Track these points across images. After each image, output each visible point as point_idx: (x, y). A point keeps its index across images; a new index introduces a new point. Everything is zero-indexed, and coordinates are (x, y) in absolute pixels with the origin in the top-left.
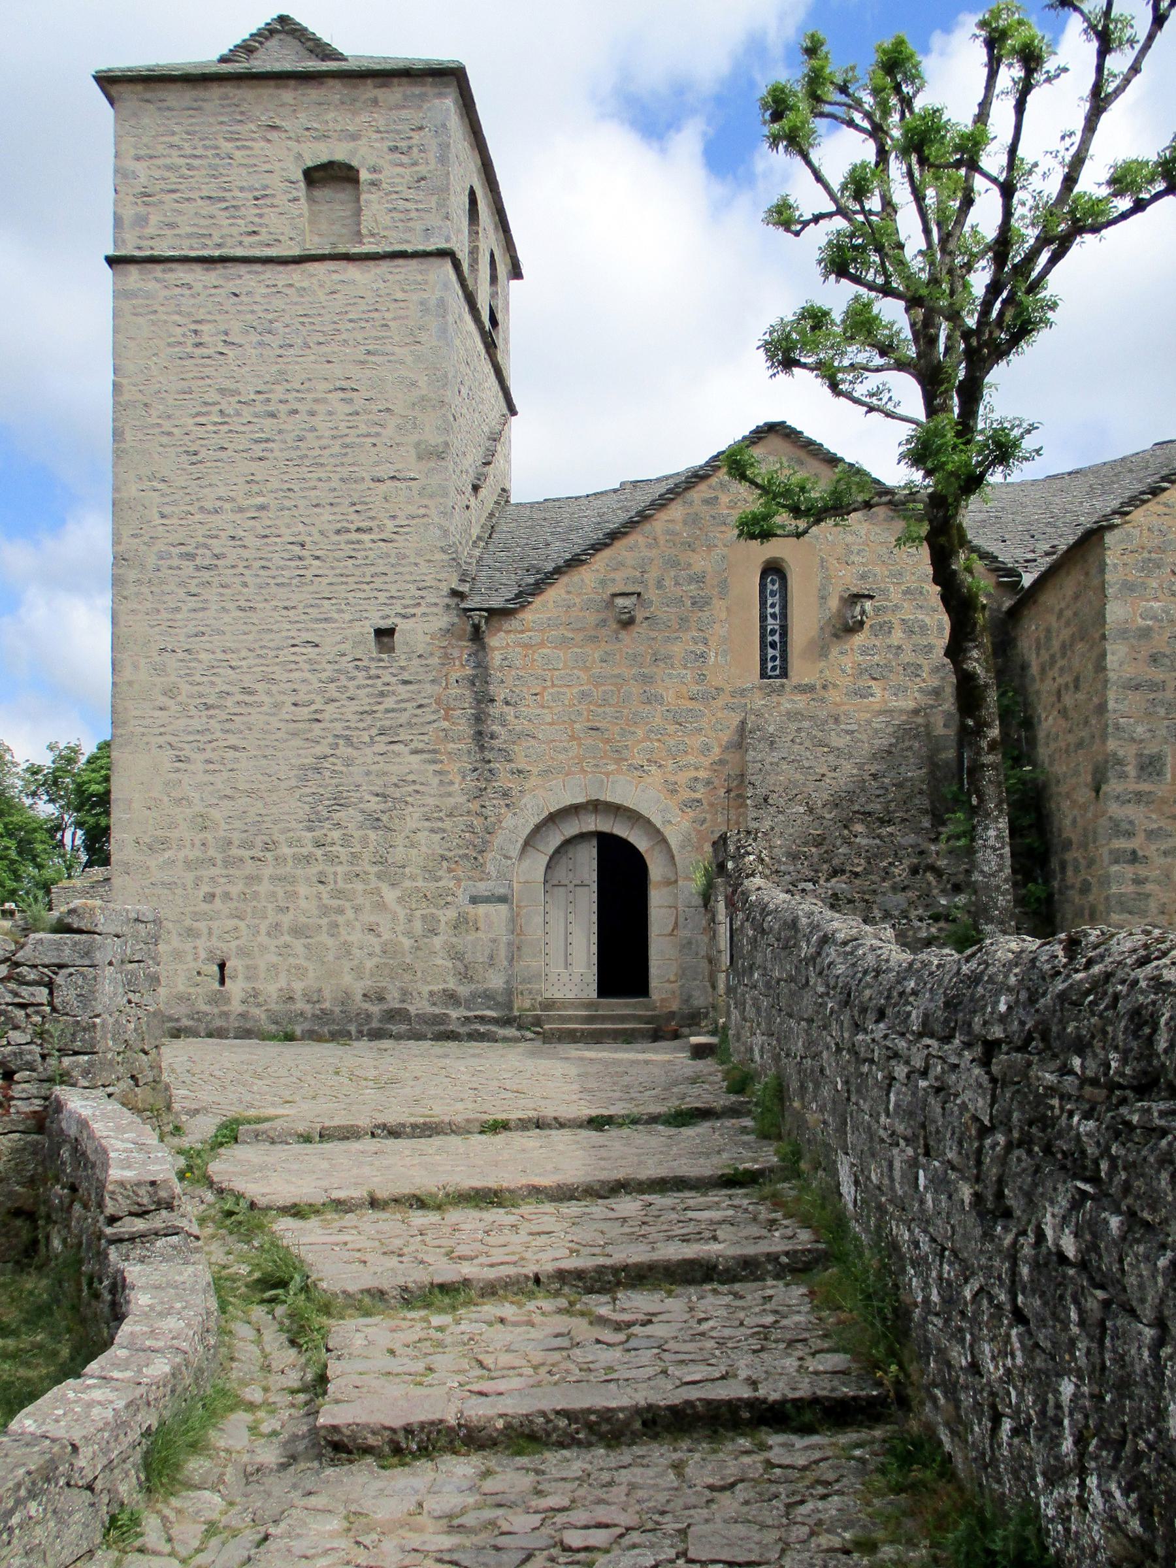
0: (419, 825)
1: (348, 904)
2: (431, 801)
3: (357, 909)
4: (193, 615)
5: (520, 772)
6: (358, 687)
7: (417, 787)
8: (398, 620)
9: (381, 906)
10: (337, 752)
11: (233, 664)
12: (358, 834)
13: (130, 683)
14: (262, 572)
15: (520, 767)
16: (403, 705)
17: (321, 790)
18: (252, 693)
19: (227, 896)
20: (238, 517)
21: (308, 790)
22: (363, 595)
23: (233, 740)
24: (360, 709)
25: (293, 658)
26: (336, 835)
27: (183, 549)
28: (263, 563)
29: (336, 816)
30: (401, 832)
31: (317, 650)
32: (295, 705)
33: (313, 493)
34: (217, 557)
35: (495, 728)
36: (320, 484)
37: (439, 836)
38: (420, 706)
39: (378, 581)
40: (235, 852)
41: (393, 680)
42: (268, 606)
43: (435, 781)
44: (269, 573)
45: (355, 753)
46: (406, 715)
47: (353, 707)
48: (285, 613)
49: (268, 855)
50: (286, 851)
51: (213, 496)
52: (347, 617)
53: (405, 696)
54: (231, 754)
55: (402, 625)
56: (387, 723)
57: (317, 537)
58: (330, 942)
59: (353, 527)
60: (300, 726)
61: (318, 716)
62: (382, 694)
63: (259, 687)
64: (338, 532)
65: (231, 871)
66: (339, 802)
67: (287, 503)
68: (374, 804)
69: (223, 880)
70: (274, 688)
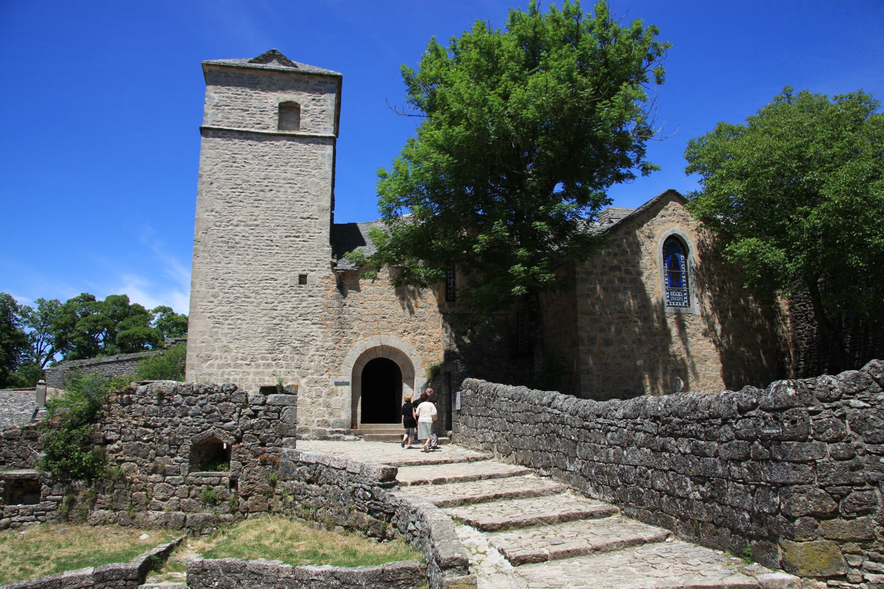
0: (315, 353)
6: (292, 297)
7: (314, 338)
10: (282, 322)
12: (289, 356)
14: (255, 250)
20: (247, 229)
21: (270, 338)
23: (240, 316)
25: (267, 285)
26: (281, 356)
29: (282, 348)
30: (307, 355)
33: (277, 221)
34: (237, 243)
39: (301, 256)
40: (239, 362)
43: (321, 336)
45: (290, 323)
47: (290, 305)
49: (253, 363)
50: (260, 362)
51: (237, 220)
53: (310, 302)
54: (239, 321)
56: (303, 312)
59: (293, 235)
62: (302, 301)
64: (286, 237)
65: (235, 370)
66: (282, 343)
68: (297, 344)
70: (258, 297)
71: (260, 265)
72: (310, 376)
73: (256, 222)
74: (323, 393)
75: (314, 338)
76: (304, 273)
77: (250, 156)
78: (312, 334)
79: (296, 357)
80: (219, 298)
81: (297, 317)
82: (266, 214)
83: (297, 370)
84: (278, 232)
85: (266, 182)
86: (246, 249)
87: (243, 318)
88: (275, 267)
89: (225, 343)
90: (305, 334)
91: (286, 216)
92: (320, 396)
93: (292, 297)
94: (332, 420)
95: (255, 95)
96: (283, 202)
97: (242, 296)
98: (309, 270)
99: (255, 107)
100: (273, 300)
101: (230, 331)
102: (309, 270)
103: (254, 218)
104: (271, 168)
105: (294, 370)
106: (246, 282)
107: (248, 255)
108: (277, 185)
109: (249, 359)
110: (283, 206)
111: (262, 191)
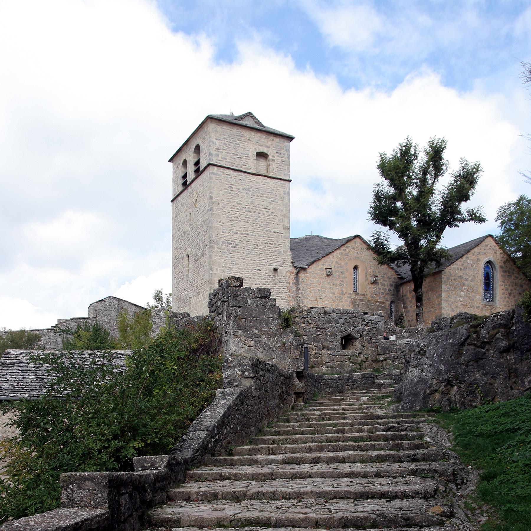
6: (270, 282)
34: (236, 245)
39: (275, 257)
42: (249, 259)
52: (268, 265)
73: (247, 232)
76: (276, 267)
77: (241, 188)
85: (251, 207)
86: (242, 249)
91: (265, 230)
93: (270, 282)
95: (241, 144)
99: (242, 153)
103: (246, 229)
107: (243, 253)
111: (250, 212)
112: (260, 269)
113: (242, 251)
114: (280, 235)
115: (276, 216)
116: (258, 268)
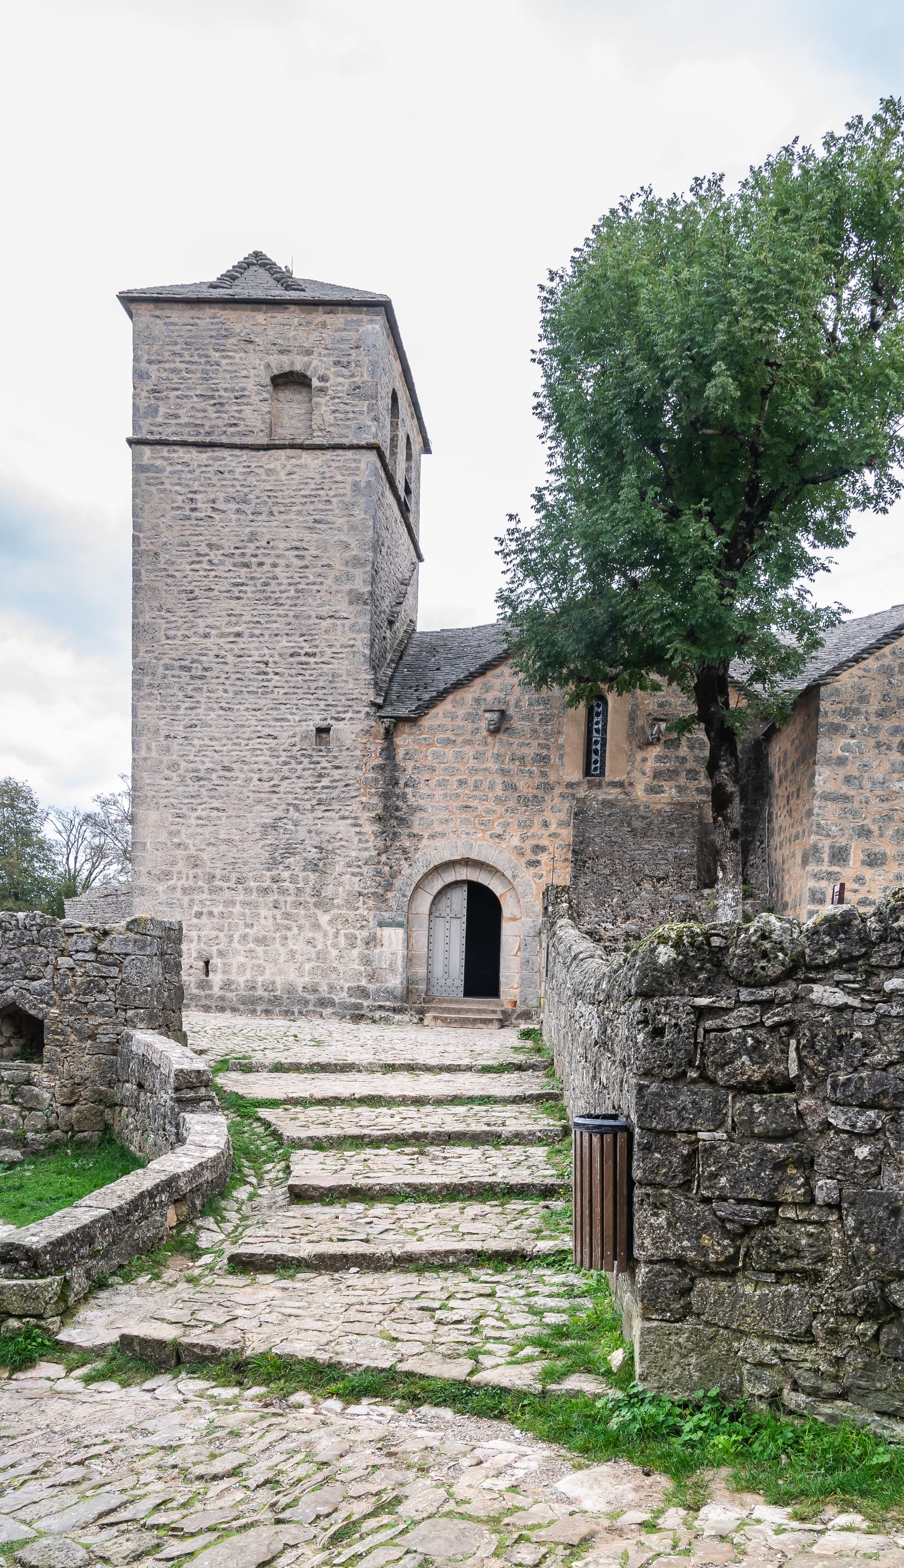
1: (294, 924)
2: (353, 854)
3: (300, 928)
4: (189, 712)
5: (415, 836)
6: (304, 770)
7: (343, 843)
8: (332, 722)
9: (316, 926)
10: (289, 816)
11: (217, 748)
12: (301, 875)
13: (145, 759)
14: (238, 682)
15: (415, 832)
16: (335, 784)
17: (277, 842)
18: (229, 769)
19: (211, 913)
20: (221, 641)
21: (268, 842)
22: (308, 702)
23: (216, 804)
24: (306, 785)
26: (286, 874)
27: (183, 663)
28: (239, 676)
29: (287, 861)
31: (275, 741)
32: (260, 780)
33: (275, 625)
35: (399, 803)
36: (279, 619)
37: (358, 878)
38: (346, 785)
39: (320, 692)
40: (218, 883)
41: (329, 765)
42: (242, 707)
43: (356, 839)
44: (243, 683)
45: (301, 817)
46: (337, 791)
47: (301, 783)
48: (254, 713)
49: (240, 886)
50: (252, 884)
52: (297, 718)
53: (337, 777)
54: (215, 813)
55: (337, 726)
56: (324, 796)
57: (277, 658)
58: (281, 950)
59: (303, 652)
60: (263, 795)
61: (275, 789)
62: (320, 776)
63: (234, 766)
64: (292, 655)
65: (214, 897)
66: (290, 851)
67: (257, 632)
68: (314, 854)
69: (208, 903)
70: (246, 767)
71: (247, 709)
72: (335, 911)
73: (237, 629)
74: (359, 941)
75: (343, 843)
76: (324, 724)
78: (339, 836)
79: (313, 877)
80: (179, 772)
81: (313, 806)
82: (255, 613)
83: (315, 899)
84: (278, 646)
85: (250, 549)
87: (224, 806)
88: (275, 713)
89: (192, 851)
90: (328, 837)
91: (291, 614)
92: (353, 946)
94: (371, 987)
96: (283, 588)
97: (218, 767)
98: (332, 718)
100: (271, 775)
101: (199, 830)
102: (332, 718)
104: (260, 518)
105: (308, 899)
106: (224, 741)
107: (226, 691)
108: (273, 552)
109: (234, 880)
110: (285, 595)
111: (246, 565)
112: (275, 734)
113: (221, 687)
114: (339, 622)
115: (329, 566)
116: (267, 731)
